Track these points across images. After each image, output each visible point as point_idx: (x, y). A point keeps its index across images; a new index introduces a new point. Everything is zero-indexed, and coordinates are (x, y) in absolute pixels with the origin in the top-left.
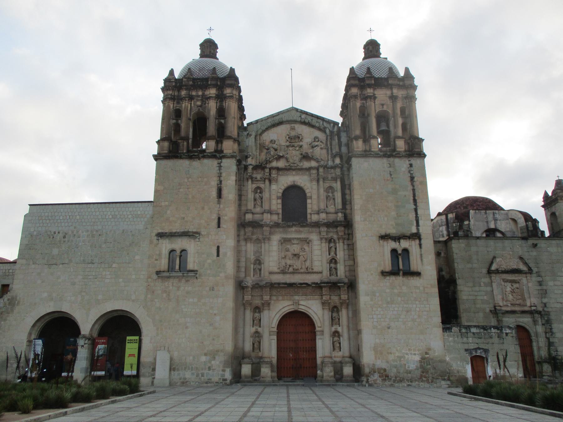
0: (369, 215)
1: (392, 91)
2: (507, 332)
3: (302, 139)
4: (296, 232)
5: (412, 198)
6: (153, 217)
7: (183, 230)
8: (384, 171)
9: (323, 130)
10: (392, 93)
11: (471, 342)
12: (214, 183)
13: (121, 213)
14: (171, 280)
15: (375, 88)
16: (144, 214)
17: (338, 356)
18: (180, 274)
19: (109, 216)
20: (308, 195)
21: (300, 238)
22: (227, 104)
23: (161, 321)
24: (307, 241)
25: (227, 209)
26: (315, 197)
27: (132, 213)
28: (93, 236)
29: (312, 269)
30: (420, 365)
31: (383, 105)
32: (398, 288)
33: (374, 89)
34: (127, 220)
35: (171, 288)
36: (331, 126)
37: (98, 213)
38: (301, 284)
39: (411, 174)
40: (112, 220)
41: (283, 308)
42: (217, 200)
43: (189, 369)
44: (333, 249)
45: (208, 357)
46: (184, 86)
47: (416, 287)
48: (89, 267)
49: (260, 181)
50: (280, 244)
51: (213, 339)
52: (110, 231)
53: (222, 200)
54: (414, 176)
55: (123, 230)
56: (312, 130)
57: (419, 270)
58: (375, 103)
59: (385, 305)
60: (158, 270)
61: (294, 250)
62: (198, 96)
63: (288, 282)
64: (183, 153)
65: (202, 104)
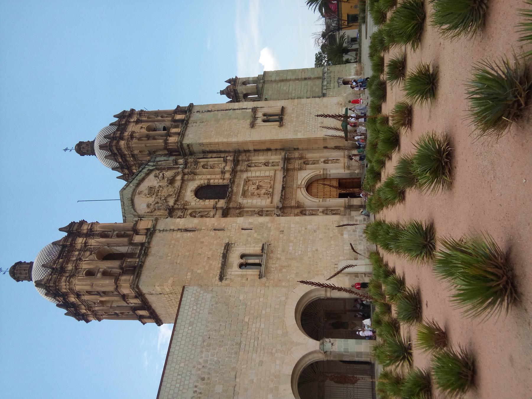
1: (132, 122)
4: (237, 187)
6: (201, 286)
7: (221, 258)
9: (150, 171)
12: (179, 234)
13: (189, 317)
14: (270, 265)
16: (195, 294)
17: (344, 161)
18: (265, 256)
19: (190, 330)
20: (206, 182)
21: (244, 184)
22: (98, 230)
23: (309, 272)
24: (247, 181)
25: (207, 224)
26: (209, 177)
27: (191, 306)
28: (209, 345)
29: (272, 176)
32: (292, 118)
34: (198, 310)
35: (277, 265)
36: (147, 167)
37: (183, 342)
38: (283, 181)
39: (205, 112)
40: (195, 326)
41: (303, 195)
42: (196, 232)
43: (356, 247)
44: (256, 164)
45: (345, 232)
46: (63, 265)
47: (293, 109)
48: (244, 347)
49: (185, 213)
51: (328, 229)
52: (207, 327)
53: (198, 227)
55: (209, 313)
56: (146, 180)
57: (281, 108)
59: (305, 125)
60: (259, 276)
61: (253, 189)
62: (79, 254)
63: (281, 189)
64: (139, 262)
65: (89, 251)
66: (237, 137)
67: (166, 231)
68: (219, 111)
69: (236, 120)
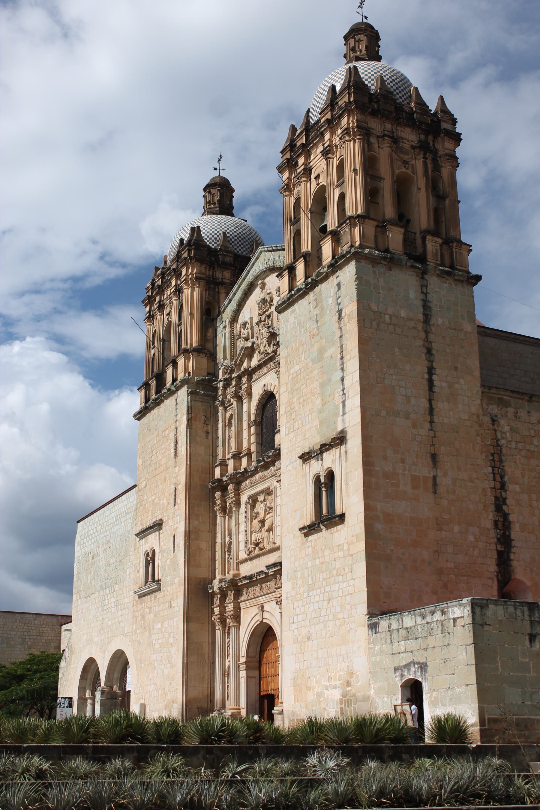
2: (456, 616)
3: (272, 301)
5: (339, 357)
8: (311, 318)
10: (323, 145)
11: (403, 649)
12: (172, 435)
30: (341, 708)
31: (317, 177)
50: (249, 506)
53: (178, 459)
58: (310, 179)
66: (288, 434)
67: (176, 409)
68: (341, 341)
69: (320, 406)
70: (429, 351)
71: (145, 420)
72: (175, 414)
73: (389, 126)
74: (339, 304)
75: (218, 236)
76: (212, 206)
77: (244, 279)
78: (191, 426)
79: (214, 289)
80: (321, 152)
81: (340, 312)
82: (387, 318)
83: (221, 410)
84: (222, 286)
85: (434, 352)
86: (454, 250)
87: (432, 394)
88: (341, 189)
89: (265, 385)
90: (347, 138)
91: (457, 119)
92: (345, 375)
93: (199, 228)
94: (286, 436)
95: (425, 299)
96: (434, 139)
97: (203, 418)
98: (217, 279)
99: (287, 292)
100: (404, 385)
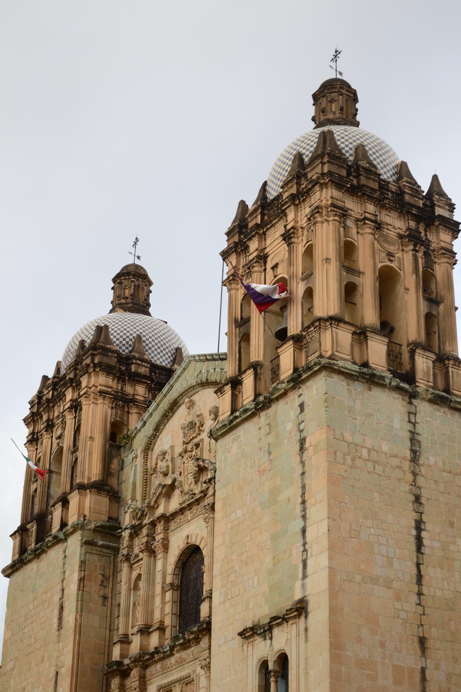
0: (231, 582)
3: (202, 426)
5: (300, 500)
8: (261, 448)
10: (285, 227)
12: (56, 599)
15: (264, 233)
21: (181, 680)
31: (275, 267)
33: (262, 237)
42: (57, 633)
53: (63, 632)
54: (305, 434)
58: (265, 270)
62: (58, 416)
66: (224, 602)
67: (64, 564)
68: (302, 480)
70: (417, 499)
71: (18, 576)
72: (62, 571)
73: (371, 208)
74: (301, 431)
75: (131, 340)
76: (124, 301)
77: (165, 396)
78: (84, 587)
79: (123, 407)
80: (282, 235)
81: (302, 442)
82: (365, 452)
83: (125, 567)
84: (134, 404)
85: (423, 500)
86: (450, 369)
87: (421, 556)
88: (307, 283)
89: (188, 536)
90: (319, 219)
91: (455, 205)
92: (307, 525)
93: (106, 327)
94: (220, 604)
95: (413, 430)
96: (426, 228)
97: (100, 577)
98: (127, 395)
99: (229, 413)
100: (385, 543)
